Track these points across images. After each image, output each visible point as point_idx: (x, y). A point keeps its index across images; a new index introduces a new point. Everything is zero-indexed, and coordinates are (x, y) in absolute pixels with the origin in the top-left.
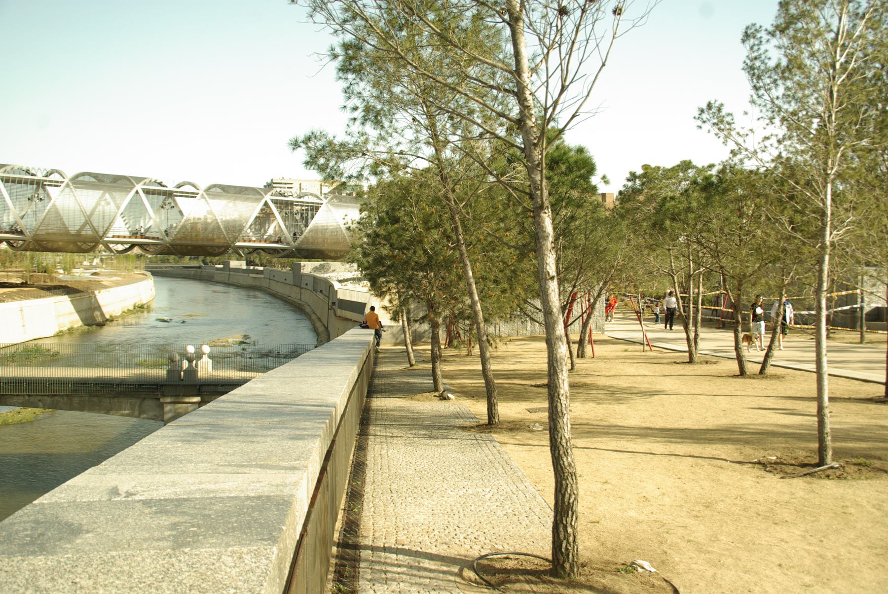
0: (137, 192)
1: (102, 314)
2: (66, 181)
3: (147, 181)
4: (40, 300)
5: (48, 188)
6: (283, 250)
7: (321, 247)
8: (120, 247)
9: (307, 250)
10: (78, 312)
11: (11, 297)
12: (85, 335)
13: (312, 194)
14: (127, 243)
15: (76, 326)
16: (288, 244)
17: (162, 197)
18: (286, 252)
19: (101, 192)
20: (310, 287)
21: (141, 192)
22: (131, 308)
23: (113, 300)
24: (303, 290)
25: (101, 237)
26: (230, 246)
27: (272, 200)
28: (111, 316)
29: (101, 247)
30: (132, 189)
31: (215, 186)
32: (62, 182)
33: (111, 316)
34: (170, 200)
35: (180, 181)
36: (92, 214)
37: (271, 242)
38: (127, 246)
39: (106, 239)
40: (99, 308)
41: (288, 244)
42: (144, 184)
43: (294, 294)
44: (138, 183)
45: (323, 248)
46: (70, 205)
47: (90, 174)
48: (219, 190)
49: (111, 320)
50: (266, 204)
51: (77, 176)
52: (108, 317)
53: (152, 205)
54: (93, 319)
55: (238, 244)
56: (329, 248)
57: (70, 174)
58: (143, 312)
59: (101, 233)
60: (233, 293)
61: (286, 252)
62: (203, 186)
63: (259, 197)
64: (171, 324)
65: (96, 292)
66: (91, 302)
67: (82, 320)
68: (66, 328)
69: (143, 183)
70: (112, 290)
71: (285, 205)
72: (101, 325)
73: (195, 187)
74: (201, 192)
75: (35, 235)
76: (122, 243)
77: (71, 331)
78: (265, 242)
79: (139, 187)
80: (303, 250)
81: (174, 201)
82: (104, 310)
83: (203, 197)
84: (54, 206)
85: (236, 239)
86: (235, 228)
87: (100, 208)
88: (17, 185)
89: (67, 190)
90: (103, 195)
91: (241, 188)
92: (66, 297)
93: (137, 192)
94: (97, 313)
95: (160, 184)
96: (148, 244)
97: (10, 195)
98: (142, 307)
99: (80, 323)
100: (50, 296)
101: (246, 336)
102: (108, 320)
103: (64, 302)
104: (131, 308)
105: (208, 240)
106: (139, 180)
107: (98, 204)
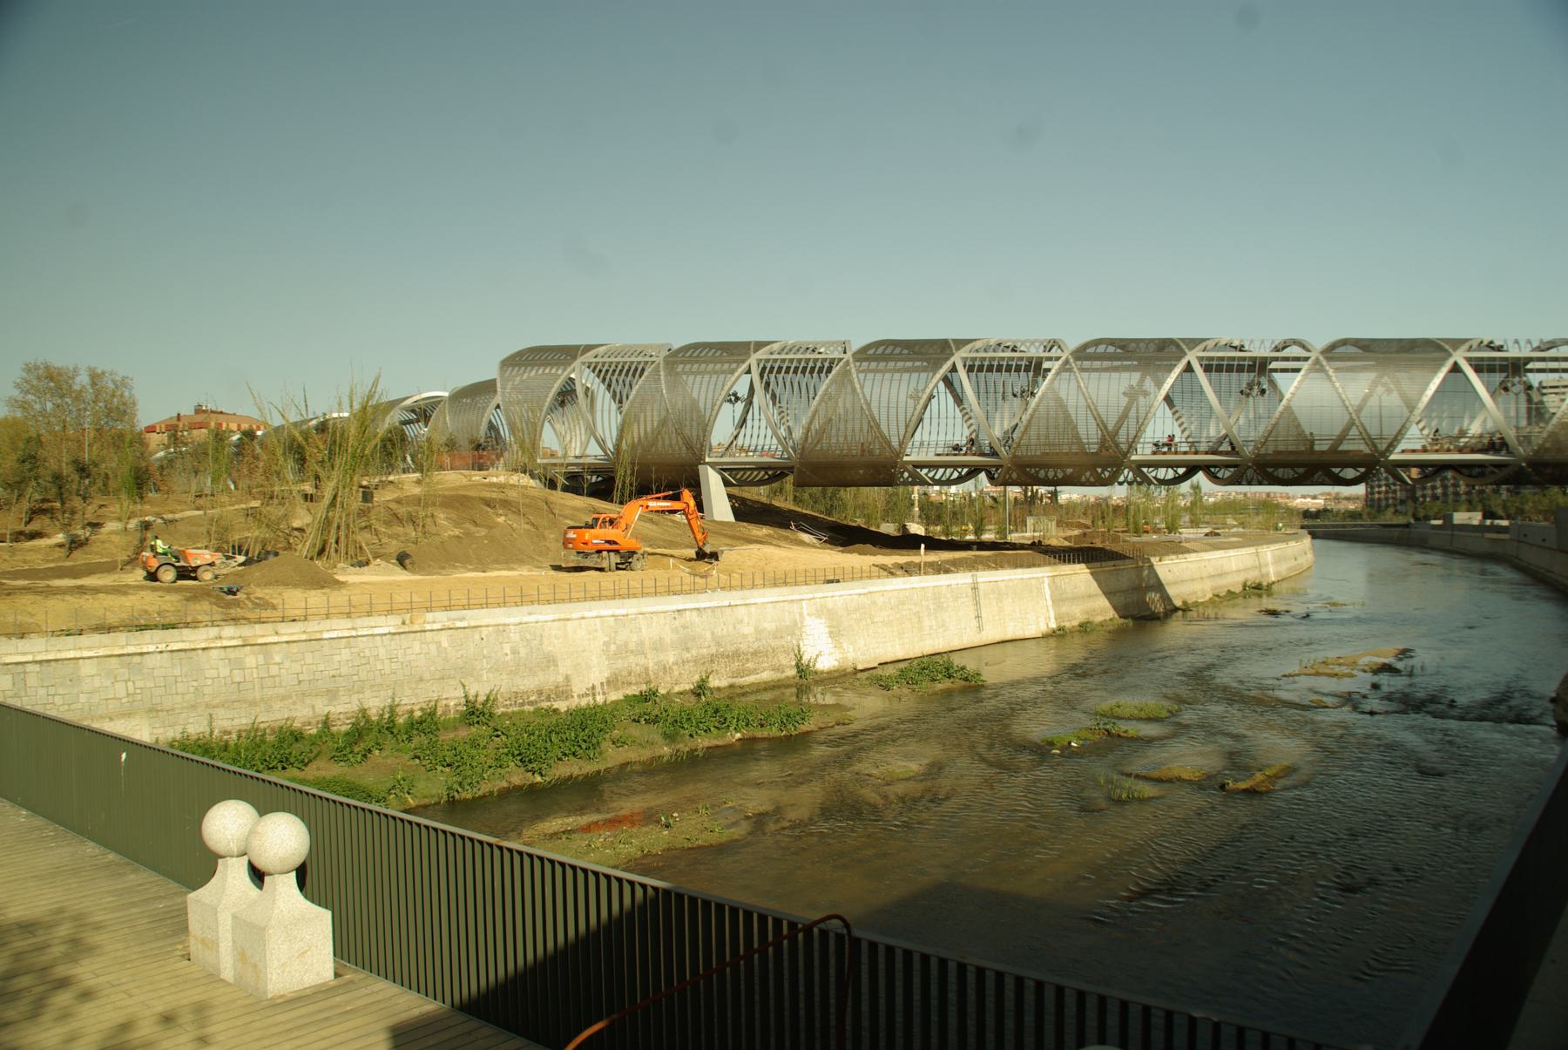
0: (1189, 368)
1: (1166, 598)
2: (1313, 355)
3: (1210, 344)
4: (1019, 571)
6: (1499, 465)
8: (1170, 474)
10: (1108, 594)
11: (971, 566)
12: (1118, 634)
14: (955, 466)
15: (1098, 619)
16: (1509, 453)
17: (1246, 377)
18: (1505, 472)
19: (1372, 375)
21: (960, 366)
22: (1238, 589)
23: (1192, 572)
25: (1125, 455)
26: (1378, 462)
27: (1469, 360)
28: (1185, 603)
29: (1127, 474)
30: (1179, 359)
31: (1344, 342)
32: (1306, 359)
33: (1185, 603)
34: (1264, 380)
35: (1548, 337)
36: (1359, 409)
37: (1473, 451)
38: (1181, 471)
39: (1392, 457)
40: (1159, 586)
42: (1470, 349)
44: (1455, 349)
46: (1089, 399)
47: (1112, 342)
48: (1351, 349)
49: (1186, 609)
50: (1456, 369)
51: (1086, 346)
52: (1178, 603)
53: (1218, 393)
54: (1143, 609)
57: (1319, 342)
58: (1260, 596)
60: (1457, 564)
63: (1437, 355)
65: (1154, 560)
67: (1115, 608)
68: (1075, 623)
69: (1202, 346)
70: (1192, 557)
72: (1154, 618)
74: (1313, 355)
75: (1015, 456)
76: (955, 466)
77: (1084, 628)
78: (1460, 451)
79: (1192, 356)
80: (1546, 465)
81: (1272, 383)
82: (1171, 591)
83: (1318, 368)
84: (1288, 408)
89: (1065, 375)
90: (1142, 381)
92: (1083, 566)
93: (1189, 368)
94: (1153, 597)
95: (1490, 346)
96: (1481, 465)
97: (1202, 392)
98: (1258, 587)
99: (1111, 613)
100: (1045, 565)
101: (1404, 653)
102: (1176, 609)
103: (1079, 576)
104: (1238, 589)
105: (1291, 452)
106: (1193, 343)
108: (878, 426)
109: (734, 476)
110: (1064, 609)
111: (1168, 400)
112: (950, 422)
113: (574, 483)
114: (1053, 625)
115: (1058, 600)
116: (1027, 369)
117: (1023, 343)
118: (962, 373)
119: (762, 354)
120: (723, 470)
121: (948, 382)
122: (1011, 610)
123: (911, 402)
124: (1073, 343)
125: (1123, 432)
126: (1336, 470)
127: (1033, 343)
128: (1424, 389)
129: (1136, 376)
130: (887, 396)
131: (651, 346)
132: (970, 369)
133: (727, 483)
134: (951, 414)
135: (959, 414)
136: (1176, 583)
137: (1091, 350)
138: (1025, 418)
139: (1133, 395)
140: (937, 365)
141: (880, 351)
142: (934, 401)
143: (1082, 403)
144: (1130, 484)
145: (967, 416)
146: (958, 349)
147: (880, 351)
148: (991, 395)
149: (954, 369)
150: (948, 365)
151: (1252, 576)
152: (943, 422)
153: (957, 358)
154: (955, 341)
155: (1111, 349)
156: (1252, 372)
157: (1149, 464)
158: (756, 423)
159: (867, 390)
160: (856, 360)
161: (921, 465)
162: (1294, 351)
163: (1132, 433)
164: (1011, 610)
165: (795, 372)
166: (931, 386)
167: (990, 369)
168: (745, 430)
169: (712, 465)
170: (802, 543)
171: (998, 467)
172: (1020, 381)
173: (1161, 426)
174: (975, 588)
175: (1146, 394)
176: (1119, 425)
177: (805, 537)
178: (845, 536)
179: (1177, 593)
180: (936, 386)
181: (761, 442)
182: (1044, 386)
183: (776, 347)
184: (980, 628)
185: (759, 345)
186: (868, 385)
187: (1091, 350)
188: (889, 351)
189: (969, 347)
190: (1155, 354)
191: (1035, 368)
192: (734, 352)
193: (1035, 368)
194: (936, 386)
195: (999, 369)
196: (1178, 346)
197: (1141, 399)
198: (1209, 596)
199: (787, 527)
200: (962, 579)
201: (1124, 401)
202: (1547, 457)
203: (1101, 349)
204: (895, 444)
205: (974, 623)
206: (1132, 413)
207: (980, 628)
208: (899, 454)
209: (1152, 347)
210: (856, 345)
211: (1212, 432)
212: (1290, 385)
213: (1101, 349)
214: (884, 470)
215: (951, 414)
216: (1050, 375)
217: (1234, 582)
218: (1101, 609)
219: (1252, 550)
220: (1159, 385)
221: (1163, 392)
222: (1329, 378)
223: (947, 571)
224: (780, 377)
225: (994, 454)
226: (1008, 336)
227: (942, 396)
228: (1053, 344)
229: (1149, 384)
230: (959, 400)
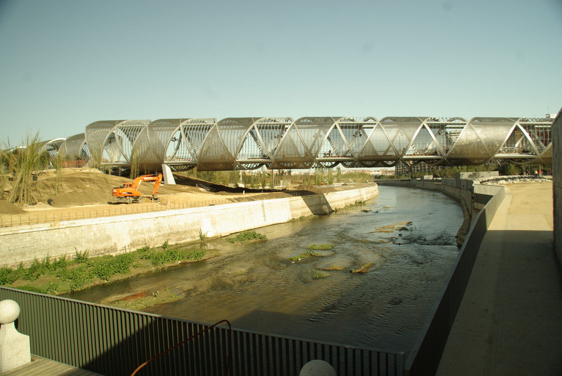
0: (335, 127)
1: (329, 207)
2: (377, 123)
3: (343, 119)
5: (365, 130)
7: (466, 156)
8: (330, 164)
9: (456, 159)
10: (309, 206)
11: (261, 198)
12: (314, 220)
13: (458, 118)
14: (255, 163)
15: (306, 215)
16: (441, 155)
17: (355, 130)
18: (440, 161)
19: (397, 129)
20: (465, 188)
21: (256, 127)
22: (354, 204)
24: (462, 190)
25: (314, 158)
26: (399, 159)
27: (428, 124)
28: (336, 209)
29: (315, 164)
30: (332, 124)
31: (387, 118)
32: (375, 124)
33: (336, 209)
34: (361, 131)
36: (393, 141)
37: (430, 155)
38: (333, 163)
40: (327, 203)
41: (441, 155)
42: (428, 120)
43: (456, 192)
44: (423, 121)
45: (468, 157)
47: (309, 118)
49: (336, 211)
50: (424, 127)
52: (333, 209)
53: (345, 136)
54: (322, 212)
55: (496, 156)
56: (473, 156)
57: (379, 118)
58: (361, 206)
59: (401, 154)
60: (426, 193)
61: (440, 161)
62: (468, 118)
63: (418, 122)
64: (369, 213)
65: (325, 194)
66: (320, 200)
68: (298, 217)
69: (340, 120)
71: (528, 127)
72: (325, 214)
73: (374, 120)
74: (377, 123)
76: (255, 163)
77: (301, 219)
78: (426, 155)
79: (336, 123)
80: (453, 159)
82: (331, 205)
84: (369, 141)
85: (495, 152)
86: (493, 147)
87: (397, 138)
88: (268, 130)
89: (293, 130)
90: (320, 131)
91: (410, 118)
93: (335, 127)
94: (325, 207)
95: (434, 120)
96: (432, 159)
97: (340, 135)
98: (360, 203)
99: (311, 213)
101: (409, 223)
102: (333, 211)
103: (299, 201)
104: (354, 204)
107: (396, 136)
108: (227, 149)
109: (175, 168)
110: (294, 212)
111: (329, 138)
112: (253, 147)
113: (116, 172)
114: (291, 218)
115: (292, 209)
116: (280, 128)
117: (278, 119)
118: (257, 130)
119: (184, 123)
120: (171, 166)
121: (251, 133)
122: (275, 213)
123: (239, 140)
124: (295, 119)
125: (313, 150)
126: (386, 162)
127: (281, 119)
128: (414, 134)
129: (317, 130)
130: (230, 138)
131: (143, 121)
132: (259, 128)
133: (172, 170)
134: (253, 144)
135: (256, 144)
136: (333, 202)
137: (302, 121)
138: (279, 145)
139: (316, 137)
140: (247, 127)
141: (227, 122)
142: (247, 140)
143: (299, 140)
144: (316, 168)
145: (258, 145)
146: (255, 121)
147: (227, 122)
148: (267, 137)
149: (254, 128)
150: (251, 127)
151: (358, 199)
152: (250, 147)
153: (255, 124)
154: (254, 118)
155: (309, 121)
156: (357, 128)
157: (323, 161)
158: (183, 148)
159: (223, 136)
160: (219, 125)
161: (243, 163)
162: (371, 121)
163: (316, 150)
164: (275, 213)
165: (197, 130)
166: (246, 134)
167: (266, 128)
168: (179, 151)
169: (167, 164)
170: (200, 192)
171: (270, 163)
172: (277, 132)
173: (326, 147)
174: (263, 206)
175: (321, 136)
176: (312, 147)
177: (202, 189)
178: (216, 189)
179: (333, 206)
180: (247, 134)
181: (185, 155)
182: (285, 134)
183: (189, 121)
184: (265, 220)
185: (183, 120)
186: (223, 134)
187: (302, 121)
188: (230, 122)
189: (259, 120)
190: (324, 122)
191: (282, 128)
192: (174, 122)
193: (282, 128)
194: (247, 134)
195: (270, 128)
196: (332, 120)
197: (319, 138)
198: (344, 206)
199: (195, 186)
200: (258, 203)
201: (313, 139)
202: (453, 157)
203: (305, 121)
204: (233, 155)
205: (263, 218)
206: (316, 143)
207: (265, 220)
208: (235, 159)
209: (323, 120)
210: (218, 120)
211: (344, 149)
212: (369, 133)
213: (305, 121)
214: (229, 165)
215: (253, 144)
216: (288, 130)
217: (352, 201)
218: (307, 212)
219: (358, 190)
220: (325, 133)
221: (327, 136)
222: (383, 130)
223: (253, 200)
224: (191, 131)
225: (269, 158)
226: (273, 116)
227: (250, 138)
228: (288, 119)
229: (322, 133)
230: (256, 139)
